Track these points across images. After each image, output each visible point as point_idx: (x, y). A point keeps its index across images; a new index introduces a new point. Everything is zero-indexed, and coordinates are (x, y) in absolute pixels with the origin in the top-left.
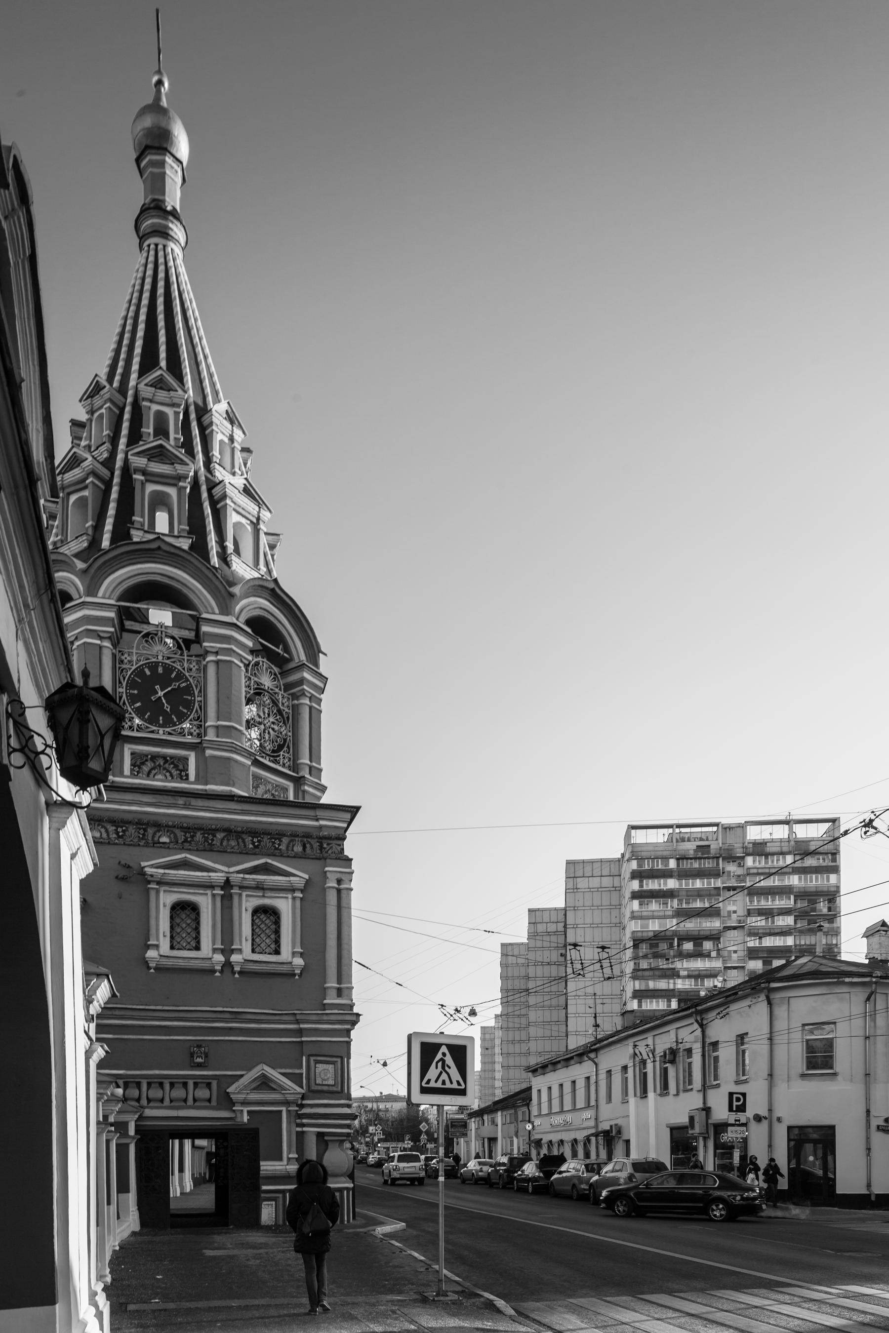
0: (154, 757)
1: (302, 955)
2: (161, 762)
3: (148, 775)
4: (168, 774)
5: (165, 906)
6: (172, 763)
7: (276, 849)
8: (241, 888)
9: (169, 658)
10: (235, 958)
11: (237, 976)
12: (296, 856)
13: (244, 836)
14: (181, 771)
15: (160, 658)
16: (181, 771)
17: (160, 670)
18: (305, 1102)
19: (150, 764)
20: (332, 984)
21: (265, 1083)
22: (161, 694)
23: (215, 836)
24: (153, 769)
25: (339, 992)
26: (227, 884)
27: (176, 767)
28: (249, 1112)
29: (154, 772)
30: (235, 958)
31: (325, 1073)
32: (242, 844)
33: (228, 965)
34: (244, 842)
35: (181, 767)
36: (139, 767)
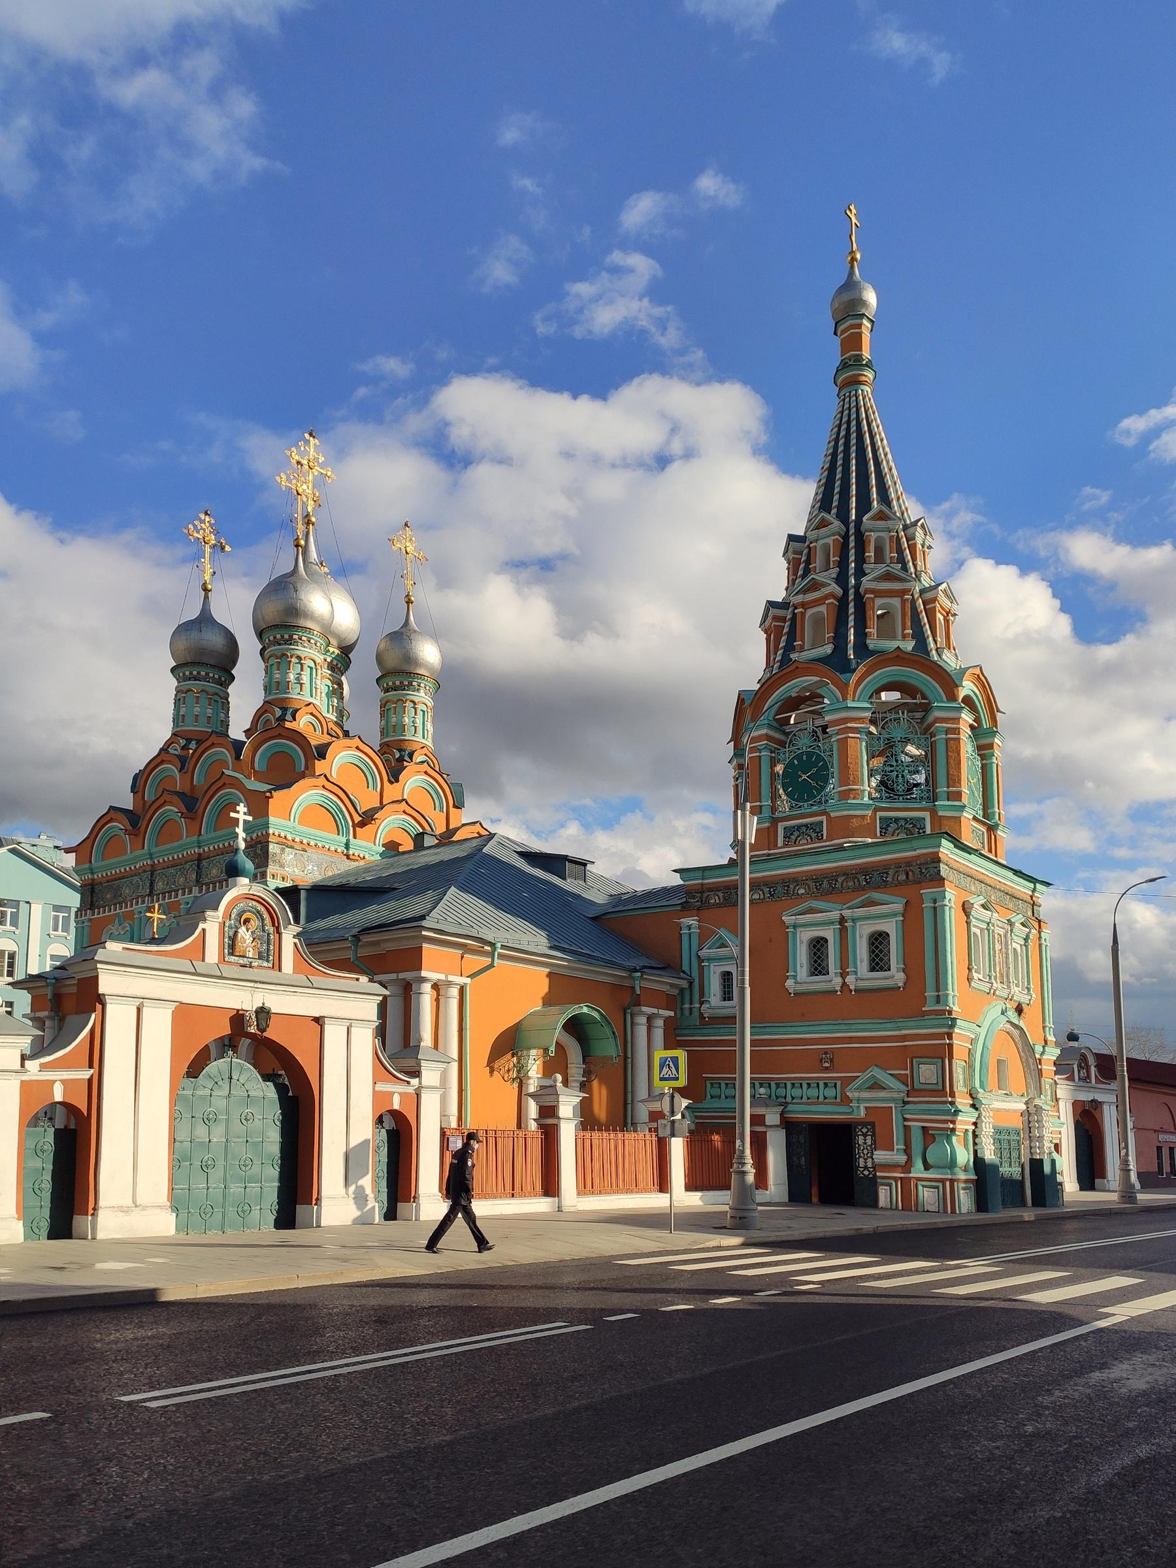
0: (799, 827)
1: (904, 970)
2: (804, 829)
3: (795, 843)
4: (809, 838)
5: (801, 942)
6: (812, 828)
7: (884, 881)
8: (854, 920)
9: (810, 747)
10: (850, 979)
11: (853, 993)
12: (899, 884)
13: (858, 876)
14: (818, 833)
15: (804, 748)
16: (818, 833)
17: (804, 758)
18: (910, 1099)
19: (796, 833)
20: (930, 993)
21: (876, 1086)
22: (804, 777)
23: (837, 881)
24: (799, 836)
25: (938, 1000)
26: (842, 920)
27: (814, 831)
28: (866, 1108)
29: (799, 838)
30: (850, 979)
31: (927, 1072)
32: (857, 883)
33: (844, 984)
34: (858, 881)
35: (818, 830)
36: (789, 838)
